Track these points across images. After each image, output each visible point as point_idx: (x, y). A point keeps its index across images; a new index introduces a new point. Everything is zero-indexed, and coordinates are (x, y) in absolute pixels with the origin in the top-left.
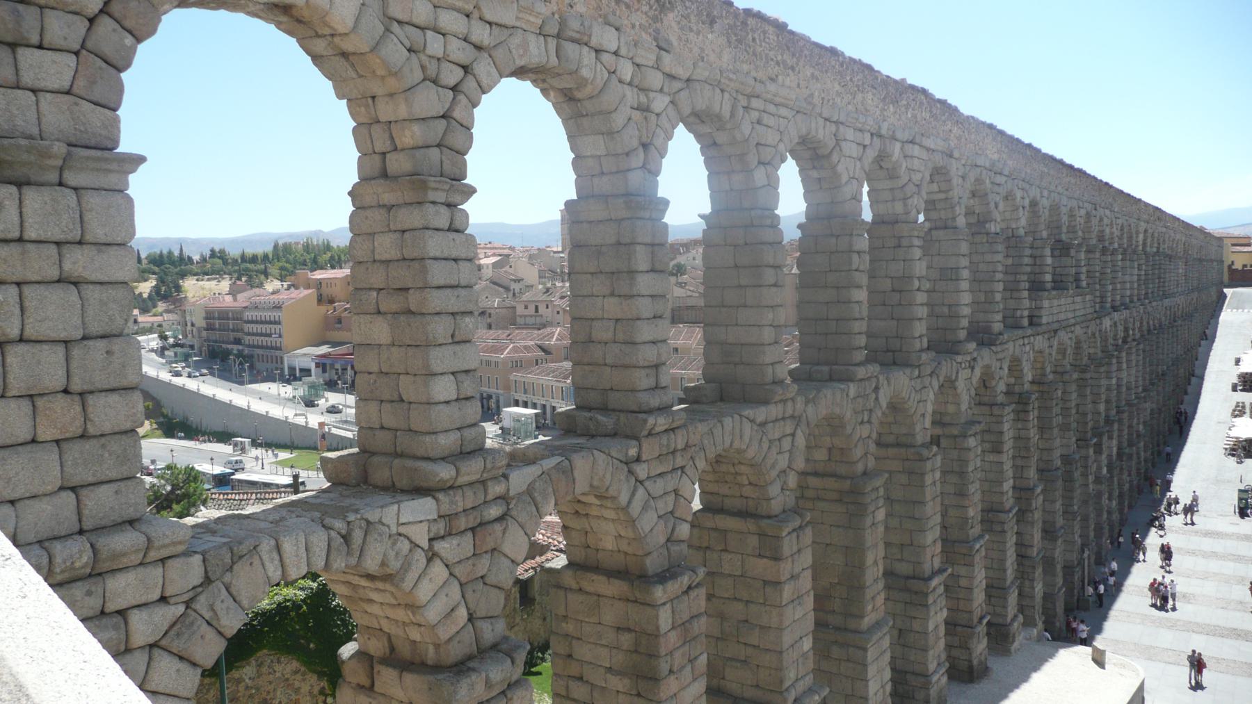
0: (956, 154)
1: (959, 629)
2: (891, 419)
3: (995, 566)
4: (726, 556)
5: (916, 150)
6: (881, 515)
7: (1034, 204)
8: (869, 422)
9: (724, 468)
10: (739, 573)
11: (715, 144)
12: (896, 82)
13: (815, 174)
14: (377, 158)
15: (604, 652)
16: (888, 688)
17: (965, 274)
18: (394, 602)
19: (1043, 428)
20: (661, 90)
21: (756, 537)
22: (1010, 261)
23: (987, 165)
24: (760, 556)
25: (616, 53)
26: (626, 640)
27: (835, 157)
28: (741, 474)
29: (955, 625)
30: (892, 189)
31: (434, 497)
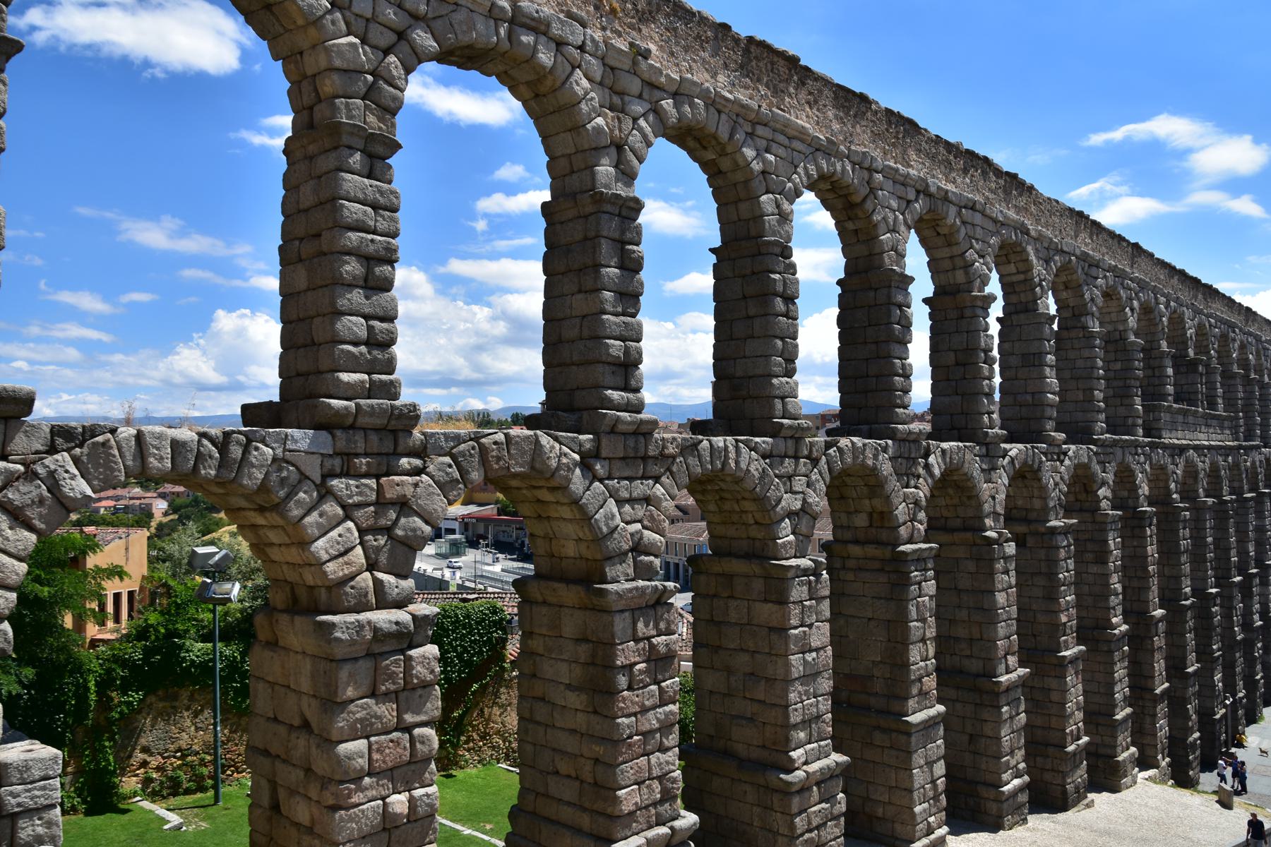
0: (1033, 233)
1: (1051, 750)
2: (956, 501)
3: (1102, 690)
5: (978, 219)
6: (930, 587)
7: (1147, 311)
8: (916, 487)
9: (727, 506)
10: (745, 621)
11: (720, 172)
12: (947, 143)
13: (850, 226)
14: (305, 113)
15: (563, 667)
16: (941, 782)
18: (287, 541)
19: (1169, 551)
20: (640, 97)
21: (761, 581)
22: (1118, 366)
23: (1078, 252)
24: (766, 601)
25: (581, 48)
26: (583, 651)
27: (869, 205)
28: (746, 512)
29: (1047, 745)
30: (951, 257)
31: (331, 433)
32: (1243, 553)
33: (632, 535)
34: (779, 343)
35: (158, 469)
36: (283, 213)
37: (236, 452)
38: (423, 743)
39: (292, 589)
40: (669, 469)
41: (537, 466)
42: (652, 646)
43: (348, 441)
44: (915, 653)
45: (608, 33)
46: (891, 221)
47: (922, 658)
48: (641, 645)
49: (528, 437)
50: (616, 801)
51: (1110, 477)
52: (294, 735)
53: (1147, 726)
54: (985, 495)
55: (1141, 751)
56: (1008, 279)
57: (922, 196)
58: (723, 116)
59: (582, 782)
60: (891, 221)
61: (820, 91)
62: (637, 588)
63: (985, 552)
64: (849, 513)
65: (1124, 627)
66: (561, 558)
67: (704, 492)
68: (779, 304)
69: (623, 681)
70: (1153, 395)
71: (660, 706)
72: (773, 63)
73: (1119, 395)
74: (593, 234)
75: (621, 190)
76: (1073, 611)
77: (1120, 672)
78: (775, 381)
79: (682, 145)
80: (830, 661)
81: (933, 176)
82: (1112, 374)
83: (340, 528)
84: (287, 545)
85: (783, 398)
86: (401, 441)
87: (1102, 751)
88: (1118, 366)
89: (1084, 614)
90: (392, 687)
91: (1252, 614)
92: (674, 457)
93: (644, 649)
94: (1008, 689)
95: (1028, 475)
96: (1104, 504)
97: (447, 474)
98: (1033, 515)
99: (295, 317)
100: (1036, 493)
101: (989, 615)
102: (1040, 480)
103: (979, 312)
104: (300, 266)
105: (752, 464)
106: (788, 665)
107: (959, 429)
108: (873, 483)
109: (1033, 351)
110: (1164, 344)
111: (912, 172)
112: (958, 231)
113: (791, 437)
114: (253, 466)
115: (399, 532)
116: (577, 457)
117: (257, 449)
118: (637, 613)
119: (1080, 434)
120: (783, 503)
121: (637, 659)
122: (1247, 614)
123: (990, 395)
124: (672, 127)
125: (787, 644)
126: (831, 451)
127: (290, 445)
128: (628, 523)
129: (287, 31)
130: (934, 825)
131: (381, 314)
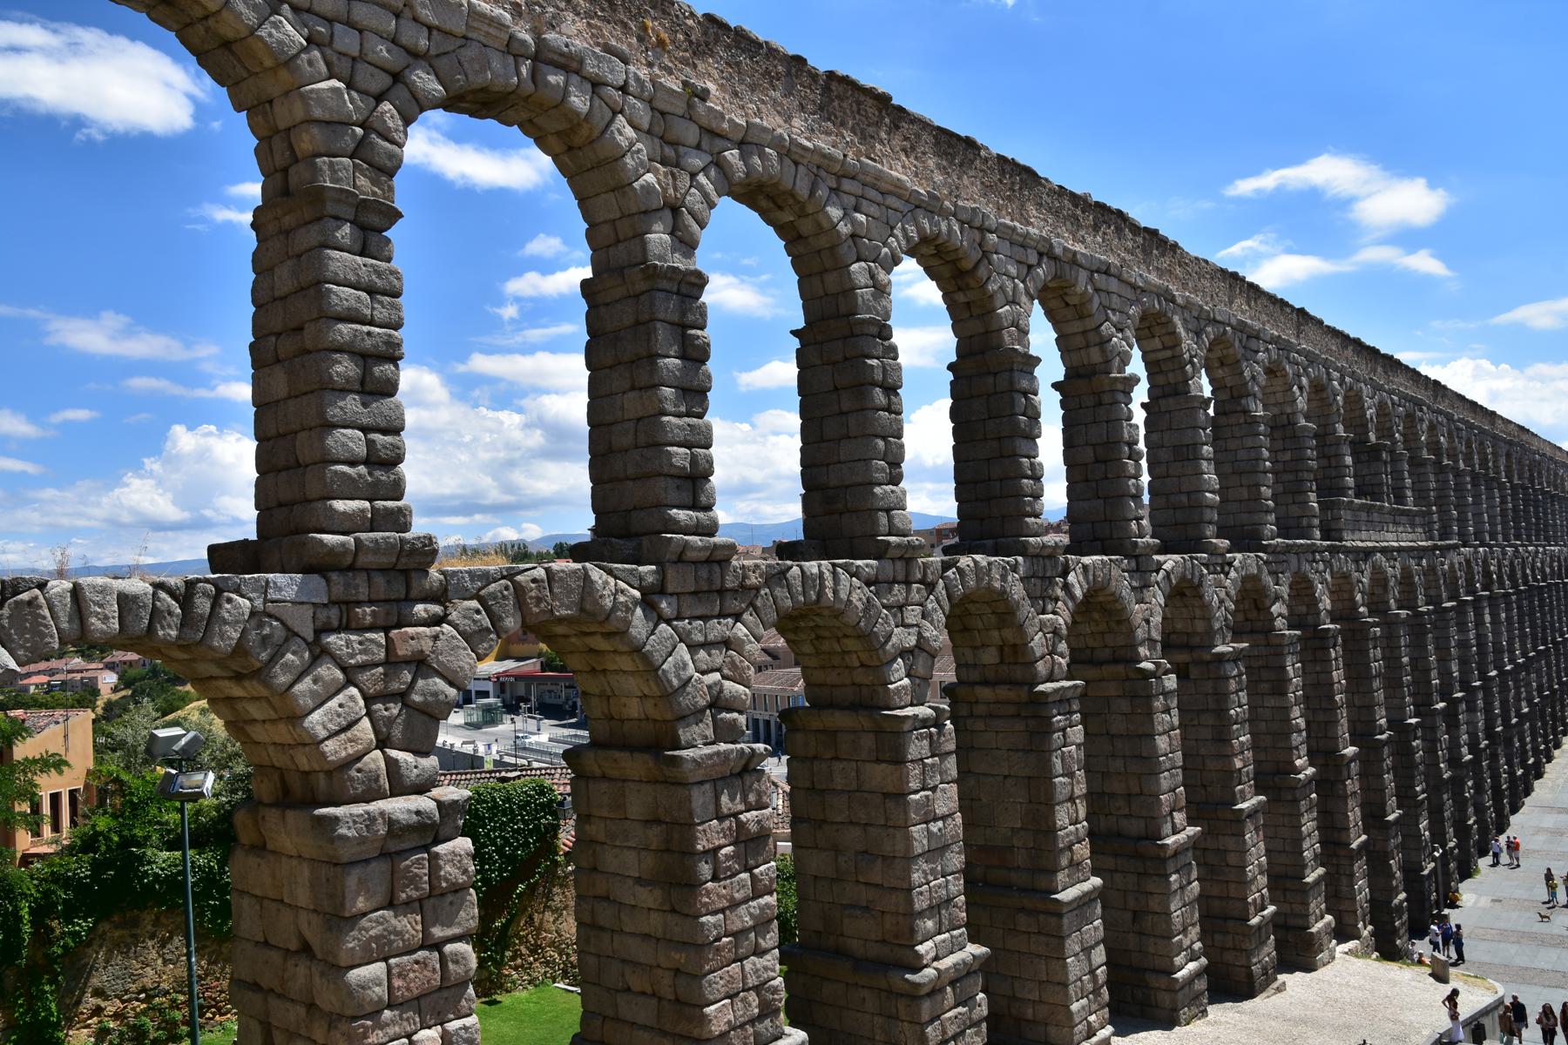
0: (1180, 300)
1: (1231, 924)
2: (1103, 627)
4: (838, 766)
5: (1113, 285)
6: (1077, 733)
8: (1054, 613)
9: (826, 646)
10: (854, 786)
11: (800, 237)
12: (1073, 196)
13: (961, 298)
14: (279, 176)
15: (630, 857)
16: (1101, 972)
17: (1207, 450)
18: (274, 716)
19: (1358, 675)
20: (698, 147)
21: (871, 736)
22: (1288, 456)
23: (1233, 321)
24: (878, 761)
25: (624, 89)
26: (654, 835)
27: (982, 272)
29: (1226, 919)
30: (1084, 332)
31: (325, 577)
32: (1445, 674)
33: (709, 687)
34: (881, 443)
35: (102, 632)
36: (254, 302)
37: (203, 605)
38: (456, 962)
39: (282, 777)
40: (752, 604)
41: (588, 607)
42: (740, 825)
43: (347, 585)
44: (1062, 816)
45: (656, 69)
46: (1009, 290)
47: (1070, 821)
48: (727, 823)
49: (575, 572)
50: (705, 1020)
51: (1284, 590)
52: (291, 962)
53: (1344, 889)
54: (1138, 619)
55: (1338, 919)
56: (1153, 356)
57: (1045, 259)
58: (801, 168)
59: (660, 999)
60: (1009, 290)
61: (918, 136)
62: (718, 753)
63: (1140, 688)
64: (975, 648)
65: (1310, 771)
66: (622, 721)
67: (796, 630)
68: (879, 396)
69: (705, 869)
70: (1330, 489)
71: (753, 899)
72: (859, 103)
73: (1290, 491)
74: (647, 317)
75: (679, 262)
76: (1249, 754)
77: (1308, 825)
78: (878, 490)
79: (753, 206)
80: (960, 831)
81: (1058, 235)
82: (1280, 466)
83: (340, 696)
84: (273, 721)
85: (888, 511)
86: (414, 584)
87: (1292, 922)
88: (1288, 456)
89: (1262, 757)
90: (415, 894)
91: (1460, 746)
92: (757, 589)
93: (730, 829)
94: (1176, 854)
95: (1187, 592)
96: (1279, 623)
97: (475, 621)
98: (1196, 640)
99: (273, 432)
100: (1198, 613)
101: (1149, 763)
102: (1201, 597)
103: (1120, 397)
104: (277, 368)
105: (853, 592)
106: (909, 839)
107: (1102, 540)
108: (1002, 610)
109: (1186, 442)
110: (1340, 428)
111: (1032, 230)
112: (1091, 300)
113: (901, 558)
114: (225, 622)
115: (417, 698)
116: (637, 594)
117: (229, 600)
118: (719, 784)
119: (1246, 540)
120: (894, 639)
121: (723, 841)
122: (1454, 746)
123: (1137, 497)
124: (740, 184)
125: (906, 813)
126: (949, 573)
127: (272, 595)
128: (703, 673)
129: (251, 74)
130: (1096, 1025)
131: (383, 424)
